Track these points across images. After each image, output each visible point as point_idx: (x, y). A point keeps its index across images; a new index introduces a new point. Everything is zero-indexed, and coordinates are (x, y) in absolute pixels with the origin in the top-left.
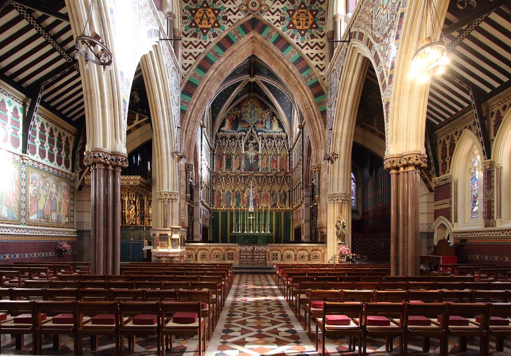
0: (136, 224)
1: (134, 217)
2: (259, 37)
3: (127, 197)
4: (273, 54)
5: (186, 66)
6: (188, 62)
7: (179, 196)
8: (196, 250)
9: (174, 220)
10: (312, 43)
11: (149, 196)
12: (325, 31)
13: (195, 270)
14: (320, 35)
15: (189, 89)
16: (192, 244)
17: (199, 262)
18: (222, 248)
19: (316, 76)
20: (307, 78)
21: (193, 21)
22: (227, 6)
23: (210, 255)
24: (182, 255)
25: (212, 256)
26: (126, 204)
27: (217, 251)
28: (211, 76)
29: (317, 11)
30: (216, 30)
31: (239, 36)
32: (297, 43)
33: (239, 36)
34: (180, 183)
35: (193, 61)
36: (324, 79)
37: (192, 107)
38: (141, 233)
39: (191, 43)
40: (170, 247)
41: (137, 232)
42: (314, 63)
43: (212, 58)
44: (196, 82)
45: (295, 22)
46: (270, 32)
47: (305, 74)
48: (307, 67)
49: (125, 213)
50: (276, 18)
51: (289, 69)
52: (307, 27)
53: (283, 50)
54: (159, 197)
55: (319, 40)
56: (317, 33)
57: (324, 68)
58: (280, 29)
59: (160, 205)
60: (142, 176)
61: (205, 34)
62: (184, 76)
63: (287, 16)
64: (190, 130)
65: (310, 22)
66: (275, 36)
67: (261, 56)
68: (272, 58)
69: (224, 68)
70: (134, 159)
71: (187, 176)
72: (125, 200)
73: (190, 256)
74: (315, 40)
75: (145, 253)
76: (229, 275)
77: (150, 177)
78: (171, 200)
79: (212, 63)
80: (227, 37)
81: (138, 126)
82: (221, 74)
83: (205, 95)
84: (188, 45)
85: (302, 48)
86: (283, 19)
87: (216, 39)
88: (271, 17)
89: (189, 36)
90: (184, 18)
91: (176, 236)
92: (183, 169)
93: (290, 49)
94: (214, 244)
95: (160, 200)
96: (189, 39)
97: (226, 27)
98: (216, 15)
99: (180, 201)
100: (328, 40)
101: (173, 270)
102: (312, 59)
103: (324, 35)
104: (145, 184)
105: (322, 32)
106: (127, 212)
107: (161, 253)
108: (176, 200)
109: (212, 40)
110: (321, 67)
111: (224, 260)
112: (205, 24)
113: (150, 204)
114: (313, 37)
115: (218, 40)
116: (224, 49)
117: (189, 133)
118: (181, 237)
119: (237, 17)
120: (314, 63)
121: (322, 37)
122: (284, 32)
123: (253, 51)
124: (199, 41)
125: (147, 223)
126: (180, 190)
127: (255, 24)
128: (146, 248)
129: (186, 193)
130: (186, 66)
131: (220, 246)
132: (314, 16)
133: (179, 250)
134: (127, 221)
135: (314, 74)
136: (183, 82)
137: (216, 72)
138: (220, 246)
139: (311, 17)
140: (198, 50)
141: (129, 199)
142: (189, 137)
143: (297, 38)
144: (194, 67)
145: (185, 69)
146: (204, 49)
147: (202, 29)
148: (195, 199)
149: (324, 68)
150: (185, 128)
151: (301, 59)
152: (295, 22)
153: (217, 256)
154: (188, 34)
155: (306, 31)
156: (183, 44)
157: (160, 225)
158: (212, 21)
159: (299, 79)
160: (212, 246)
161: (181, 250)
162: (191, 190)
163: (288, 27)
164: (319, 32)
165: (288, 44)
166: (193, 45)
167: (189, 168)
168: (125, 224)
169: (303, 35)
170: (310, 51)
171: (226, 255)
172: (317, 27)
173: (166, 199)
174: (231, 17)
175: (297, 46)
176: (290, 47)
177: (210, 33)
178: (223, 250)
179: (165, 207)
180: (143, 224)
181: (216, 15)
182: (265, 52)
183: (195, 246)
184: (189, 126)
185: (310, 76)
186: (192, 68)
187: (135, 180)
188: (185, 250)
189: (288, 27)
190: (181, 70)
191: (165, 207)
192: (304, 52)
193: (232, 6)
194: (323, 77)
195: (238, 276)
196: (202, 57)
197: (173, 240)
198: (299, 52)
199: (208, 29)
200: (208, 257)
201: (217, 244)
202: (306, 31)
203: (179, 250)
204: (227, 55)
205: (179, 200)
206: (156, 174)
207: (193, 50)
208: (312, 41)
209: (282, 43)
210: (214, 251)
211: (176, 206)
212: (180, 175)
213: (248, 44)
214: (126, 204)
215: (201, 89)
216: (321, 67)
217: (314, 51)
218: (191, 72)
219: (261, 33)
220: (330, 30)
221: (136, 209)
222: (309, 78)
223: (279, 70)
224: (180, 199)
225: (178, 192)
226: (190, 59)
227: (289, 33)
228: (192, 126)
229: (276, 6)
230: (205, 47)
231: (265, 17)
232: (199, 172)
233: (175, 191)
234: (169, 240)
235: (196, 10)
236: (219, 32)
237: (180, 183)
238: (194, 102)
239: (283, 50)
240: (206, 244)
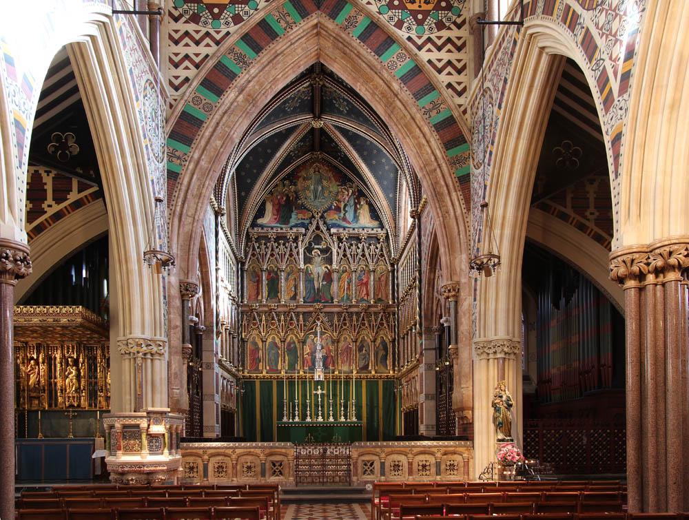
0: (79, 406)
1: (76, 391)
2: (330, 24)
3: (59, 352)
4: (360, 61)
5: (177, 82)
6: (182, 73)
7: (167, 348)
8: (206, 457)
9: (158, 397)
10: (439, 38)
11: (105, 349)
13: (193, 502)
14: (455, 23)
15: (183, 129)
16: (197, 444)
17: (213, 480)
18: (258, 451)
19: (449, 106)
20: (430, 110)
23: (234, 467)
24: (173, 467)
25: (238, 467)
26: (58, 365)
27: (249, 458)
28: (232, 104)
31: (287, 23)
32: (409, 39)
33: (287, 23)
34: (170, 321)
35: (191, 73)
36: (465, 112)
37: (191, 167)
38: (91, 424)
39: (187, 34)
40: (146, 451)
41: (81, 422)
42: (443, 79)
43: (231, 65)
44: (198, 113)
46: (353, 14)
47: (425, 101)
48: (430, 87)
49: (56, 384)
51: (391, 90)
52: (430, 7)
53: (379, 51)
54: (123, 349)
55: (454, 33)
56: (449, 19)
57: (465, 89)
59: (127, 365)
60: (87, 307)
61: (216, 17)
62: (173, 102)
64: (190, 214)
66: (362, 23)
67: (336, 65)
68: (356, 69)
69: (257, 87)
70: (73, 273)
71: (183, 307)
72: (55, 358)
73: (192, 469)
74: (445, 34)
75: (98, 463)
76: (271, 509)
77: (107, 310)
78: (149, 356)
79: (232, 76)
80: (263, 24)
81: (77, 205)
82: (251, 99)
83: (219, 143)
84: (181, 38)
85: (420, 48)
87: (241, 27)
89: (183, 19)
91: (159, 429)
92: (175, 292)
93: (394, 50)
94: (243, 444)
95: (127, 356)
96: (182, 26)
99: (170, 357)
100: (472, 31)
101: (142, 503)
102: (440, 71)
103: (464, 22)
104: (96, 323)
105: (459, 16)
106: (59, 381)
107: (124, 464)
108: (160, 355)
109: (233, 28)
110: (459, 88)
111: (263, 474)
113: (108, 366)
114: (440, 26)
115: (245, 30)
116: (257, 49)
117: (187, 220)
118: (170, 430)
120: (443, 79)
121: (459, 26)
122: (381, 16)
123: (318, 56)
124: (204, 30)
125: (104, 403)
126: (168, 335)
128: (97, 454)
129: (183, 342)
130: (177, 82)
131: (255, 448)
133: (165, 457)
134: (60, 400)
135: (444, 102)
136: (173, 113)
137: (241, 96)
138: (255, 448)
140: (203, 50)
141: (64, 356)
142: (187, 228)
143: (409, 29)
144: (195, 84)
145: (177, 88)
146: (215, 47)
148: (205, 356)
149: (465, 89)
150: (178, 209)
151: (417, 70)
153: (249, 468)
154: (181, 16)
155: (426, 14)
156: (171, 37)
157: (128, 407)
159: (414, 110)
160: (237, 448)
161: (171, 458)
162: (196, 339)
164: (454, 17)
165: (390, 41)
166: (192, 38)
167: (187, 290)
168: (56, 405)
169: (420, 23)
170: (435, 55)
171: (268, 466)
173: (138, 352)
175: (410, 45)
176: (395, 46)
177: (227, 14)
178: (262, 457)
179: (138, 369)
180: (96, 406)
182: (342, 58)
183: (203, 448)
184: (186, 205)
185: (435, 106)
186: (189, 86)
187: (71, 314)
188: (178, 457)
190: (169, 91)
191: (138, 369)
192: (424, 56)
194: (462, 109)
195: (292, 509)
196: (210, 64)
197: (152, 437)
198: (414, 57)
200: (230, 471)
201: (248, 444)
203: (165, 457)
204: (265, 60)
205: (166, 355)
206: (117, 303)
207: (192, 50)
208: (439, 34)
209: (377, 38)
210: (242, 459)
211: (160, 367)
212: (168, 304)
213: (308, 40)
214: (58, 365)
215: (210, 129)
216: (459, 88)
217: (444, 56)
218: (188, 94)
219: (333, 15)
220: (477, 11)
221: (78, 377)
222: (433, 108)
223: (373, 94)
224: (170, 353)
225: (166, 339)
226: (187, 68)
227: (391, 18)
228: (193, 205)
230: (218, 43)
232: (213, 302)
233: (158, 337)
234: (144, 436)
236: (246, 13)
237: (170, 321)
238: (196, 156)
240: (225, 444)
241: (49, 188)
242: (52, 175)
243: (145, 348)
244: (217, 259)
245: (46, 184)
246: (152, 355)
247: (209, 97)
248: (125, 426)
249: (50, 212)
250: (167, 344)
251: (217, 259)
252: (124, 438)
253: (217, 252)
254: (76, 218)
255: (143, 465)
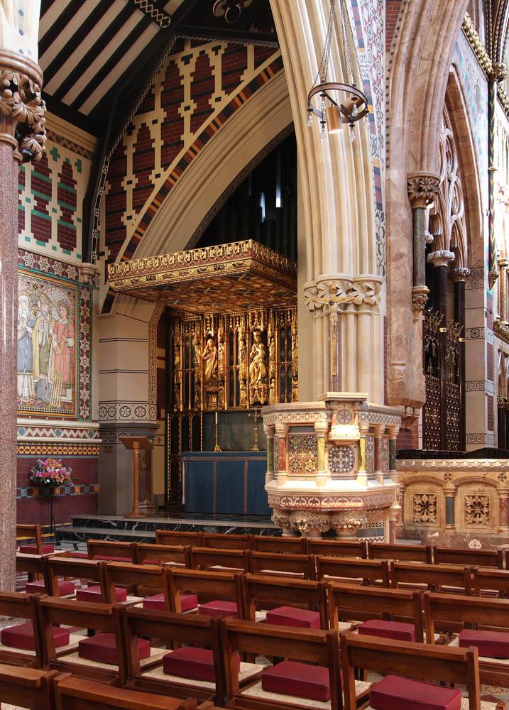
7: (383, 294)
78: (351, 309)
99: (388, 309)
108: (371, 306)
129: (414, 283)
133: (360, 483)
161: (373, 485)
203: (360, 483)
205: (382, 306)
211: (371, 329)
225: (380, 278)
233: (366, 275)
241: (217, 73)
242: (221, 52)
243: (344, 295)
244: (490, 154)
245: (213, 68)
246: (357, 306)
248: (291, 428)
249: (218, 108)
250: (383, 287)
251: (490, 154)
252: (291, 449)
253: (490, 142)
254: (252, 108)
255: (319, 497)
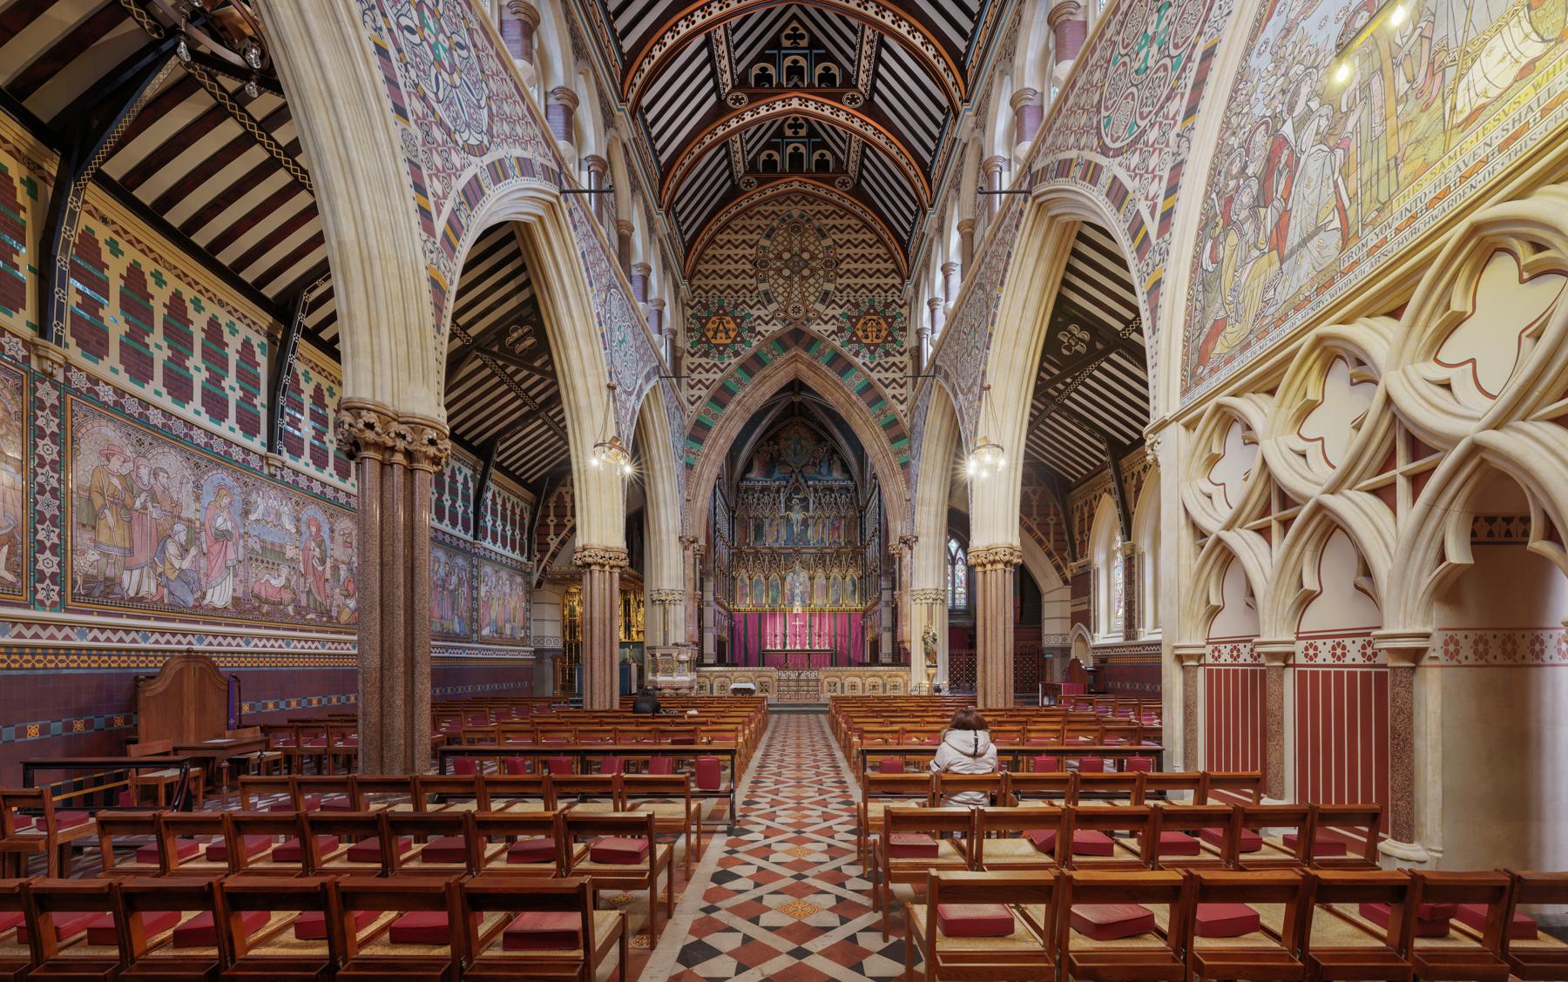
2: (805, 355)
6: (696, 393)
12: (907, 345)
21: (704, 335)
22: (755, 313)
29: (894, 318)
30: (737, 346)
35: (704, 393)
42: (889, 392)
43: (731, 384)
44: (707, 420)
45: (860, 333)
47: (875, 409)
48: (879, 398)
50: (830, 327)
53: (841, 374)
55: (897, 359)
58: (837, 343)
61: (721, 353)
63: (848, 325)
65: (884, 333)
74: (891, 359)
79: (733, 394)
86: (841, 329)
88: (823, 327)
90: (690, 330)
96: (697, 360)
97: (755, 343)
98: (739, 325)
102: (887, 386)
109: (734, 360)
112: (721, 339)
114: (887, 354)
116: (751, 374)
119: (770, 328)
120: (889, 392)
127: (797, 337)
132: (890, 325)
139: (884, 326)
140: (711, 376)
147: (717, 346)
152: (860, 333)
155: (876, 346)
158: (732, 334)
163: (850, 341)
165: (849, 366)
169: (872, 353)
170: (883, 375)
172: (894, 341)
174: (762, 328)
181: (739, 325)
189: (850, 341)
192: (875, 376)
193: (762, 313)
196: (716, 386)
199: (726, 346)
202: (876, 346)
219: (807, 349)
229: (830, 312)
231: (814, 328)
235: (708, 319)
239: (841, 374)
247: (716, 410)
